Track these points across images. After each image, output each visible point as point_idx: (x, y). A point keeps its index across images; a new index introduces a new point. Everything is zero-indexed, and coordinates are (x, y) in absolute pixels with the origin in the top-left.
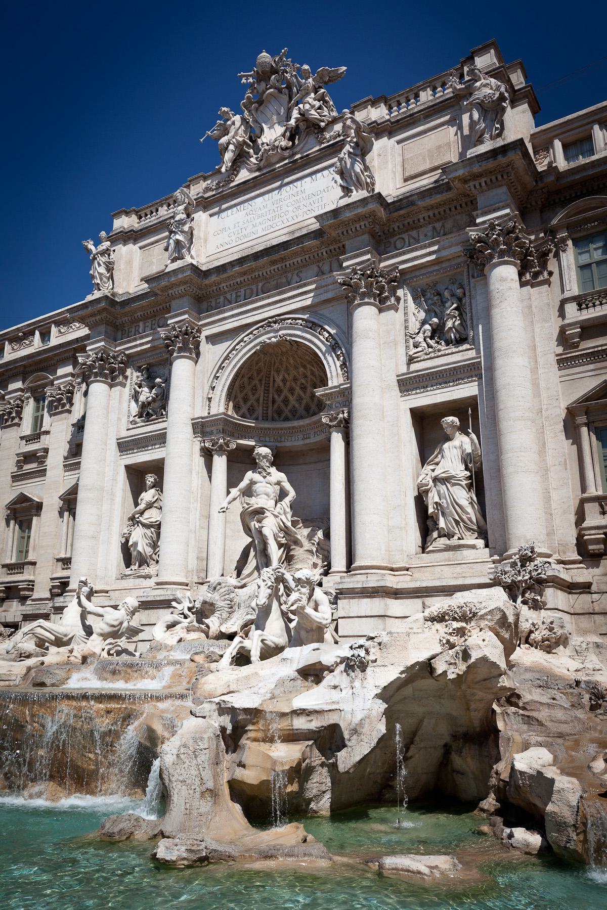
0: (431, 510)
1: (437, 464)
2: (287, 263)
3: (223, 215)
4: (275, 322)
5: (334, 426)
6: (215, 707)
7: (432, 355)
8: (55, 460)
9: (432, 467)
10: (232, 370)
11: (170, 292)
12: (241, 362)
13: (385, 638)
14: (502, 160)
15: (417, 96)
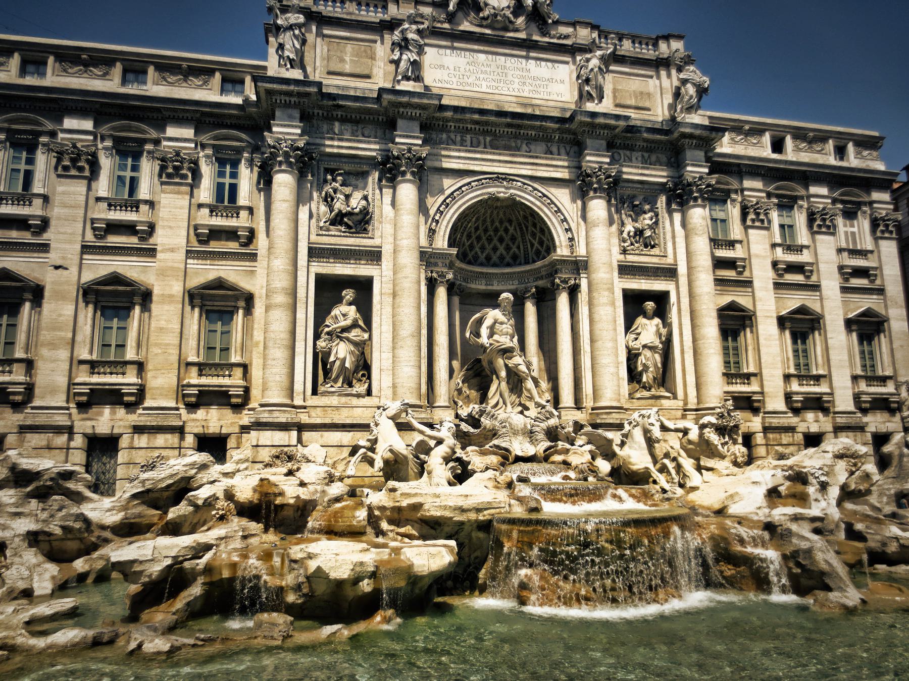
0: (640, 368)
1: (639, 334)
2: (522, 132)
3: (442, 51)
4: (503, 179)
5: (564, 288)
6: (788, 518)
7: (637, 252)
8: (172, 237)
9: (634, 336)
10: (457, 210)
11: (401, 110)
12: (467, 205)
13: (826, 469)
14: (714, 135)
15: (620, 40)
